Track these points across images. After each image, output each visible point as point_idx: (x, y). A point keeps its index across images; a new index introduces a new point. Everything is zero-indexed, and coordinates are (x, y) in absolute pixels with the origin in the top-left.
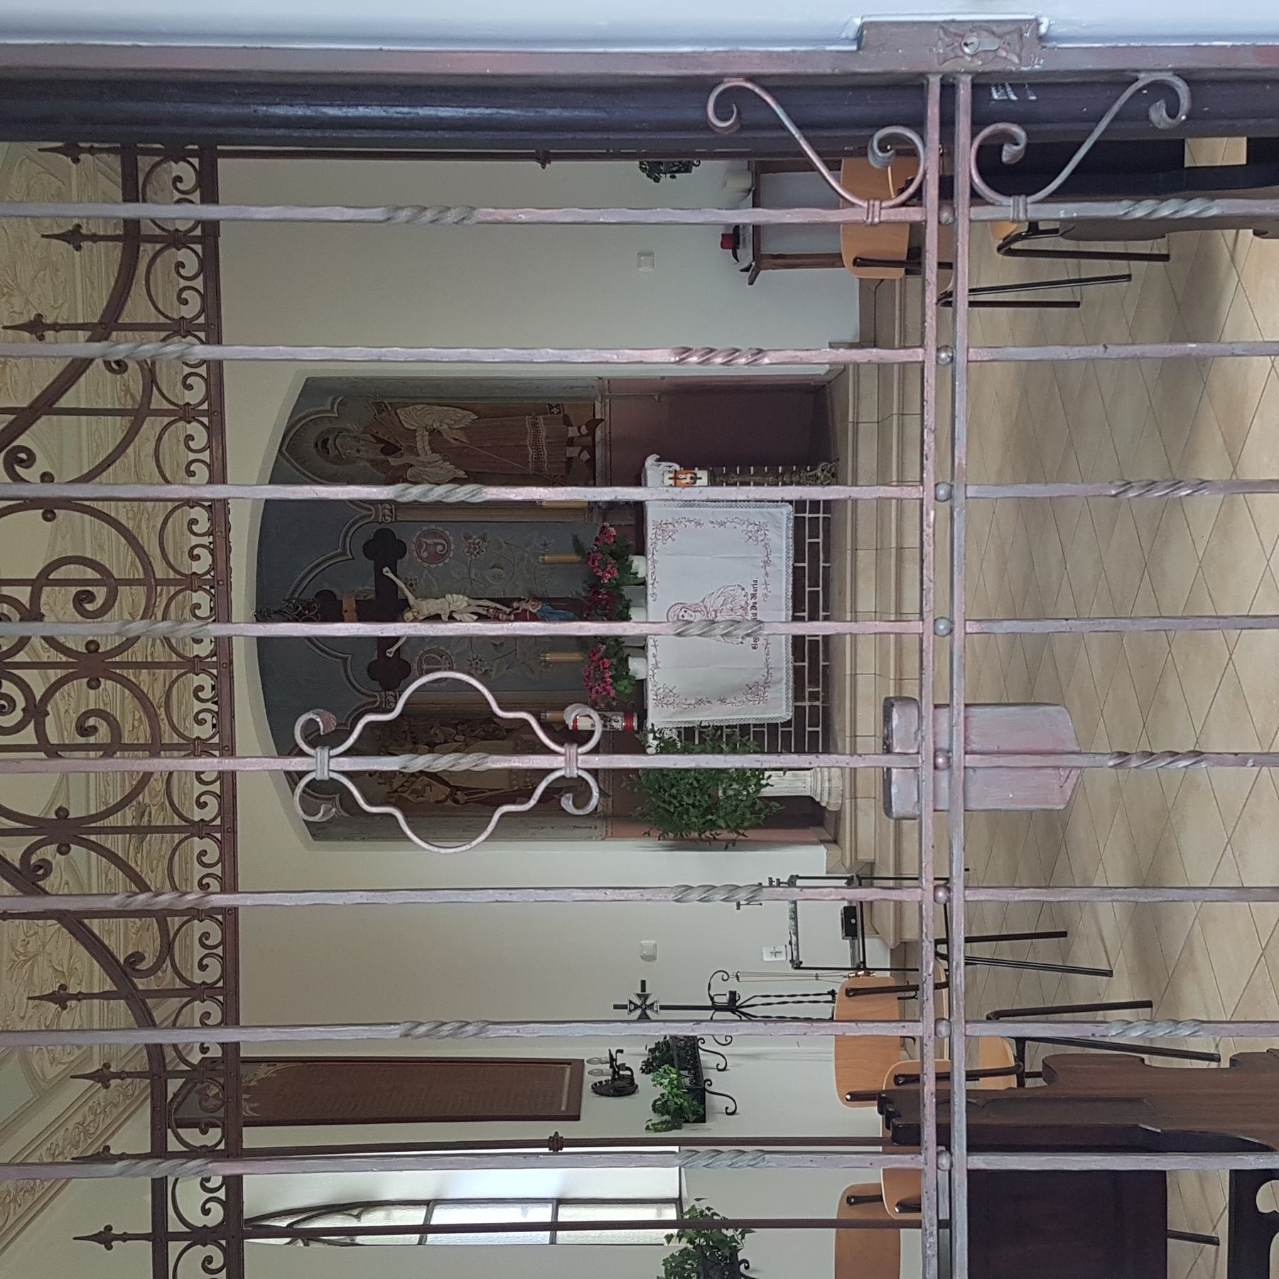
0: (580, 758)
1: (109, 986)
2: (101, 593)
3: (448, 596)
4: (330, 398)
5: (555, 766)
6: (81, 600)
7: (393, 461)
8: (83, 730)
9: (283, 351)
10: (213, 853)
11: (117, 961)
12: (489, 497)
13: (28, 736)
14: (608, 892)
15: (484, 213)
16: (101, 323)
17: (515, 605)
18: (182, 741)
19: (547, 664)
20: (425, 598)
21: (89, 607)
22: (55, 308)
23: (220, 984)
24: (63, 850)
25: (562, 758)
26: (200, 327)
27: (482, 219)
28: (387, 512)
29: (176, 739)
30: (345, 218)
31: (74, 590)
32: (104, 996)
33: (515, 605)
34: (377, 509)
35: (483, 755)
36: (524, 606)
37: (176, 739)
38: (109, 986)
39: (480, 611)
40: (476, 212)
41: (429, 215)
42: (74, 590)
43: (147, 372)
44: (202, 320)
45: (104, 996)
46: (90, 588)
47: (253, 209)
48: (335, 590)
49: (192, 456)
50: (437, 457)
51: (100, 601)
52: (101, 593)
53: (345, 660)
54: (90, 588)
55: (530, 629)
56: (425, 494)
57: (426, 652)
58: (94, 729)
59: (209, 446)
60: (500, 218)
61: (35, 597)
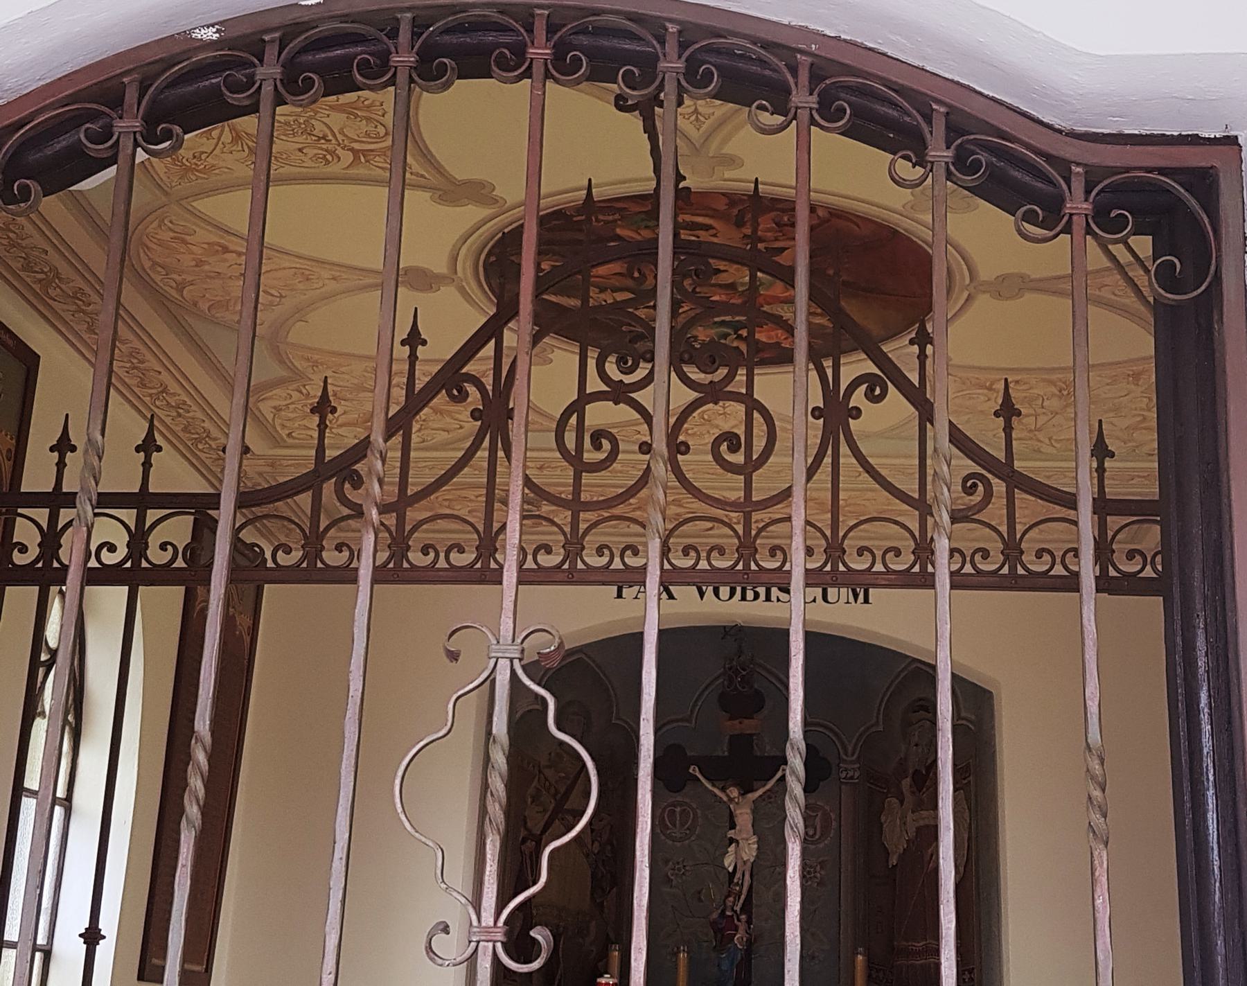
0: (491, 944)
1: (330, 454)
2: (738, 458)
3: (755, 839)
4: (973, 717)
5: (483, 914)
6: (731, 439)
7: (906, 783)
8: (597, 436)
9: (945, 630)
10: (459, 559)
11: (357, 462)
12: (790, 845)
13: (594, 384)
14: (332, 977)
15: (1102, 856)
16: (1014, 471)
17: (743, 917)
18: (581, 531)
19: (676, 954)
20: (754, 812)
21: (724, 447)
22: (1050, 439)
23: (319, 565)
24: (475, 414)
25: (492, 924)
26: (1013, 569)
27: (1096, 853)
28: (851, 774)
29: (583, 526)
30: (1089, 703)
31: (741, 431)
32: (321, 449)
33: (743, 917)
34: (852, 762)
35: (502, 828)
36: (742, 928)
37: (583, 526)
38: (330, 454)
39: (738, 875)
40: (1102, 846)
41: (1097, 793)
42: (741, 431)
43: (964, 513)
44: (1021, 571)
45: (321, 449)
46: (743, 449)
47: (1092, 607)
48: (765, 711)
49: (879, 554)
50: (912, 833)
51: (730, 458)
52: (738, 458)
53: (689, 721)
54: (743, 449)
55: (641, 887)
56: (793, 772)
57: (695, 815)
58: (597, 447)
59: (889, 571)
60: (1097, 874)
61: (736, 397)
